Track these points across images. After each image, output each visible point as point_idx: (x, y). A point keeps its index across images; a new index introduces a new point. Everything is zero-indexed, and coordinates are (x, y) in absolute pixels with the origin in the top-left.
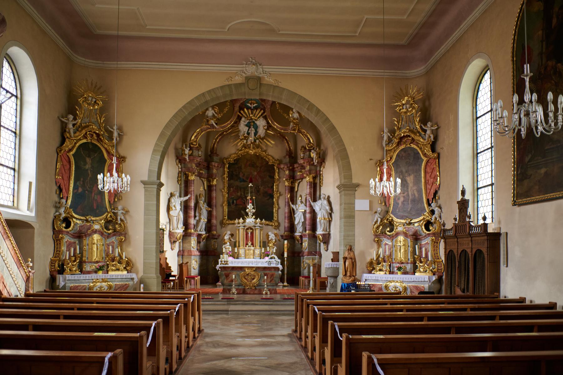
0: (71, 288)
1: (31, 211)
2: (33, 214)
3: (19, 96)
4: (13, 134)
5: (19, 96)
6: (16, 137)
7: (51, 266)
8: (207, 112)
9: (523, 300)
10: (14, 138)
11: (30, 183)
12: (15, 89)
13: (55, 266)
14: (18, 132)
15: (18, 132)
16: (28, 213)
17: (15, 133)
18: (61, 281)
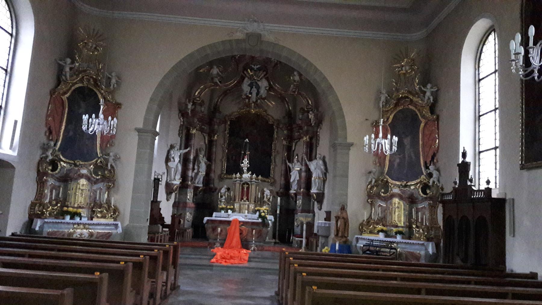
0: (48, 233)
1: (14, 151)
2: (15, 154)
3: (14, 34)
4: (4, 72)
5: (14, 34)
6: (6, 75)
7: (31, 209)
8: (212, 70)
9: (534, 276)
10: (5, 75)
11: (16, 122)
12: (11, 28)
13: (34, 209)
14: (9, 70)
15: (9, 70)
16: (10, 152)
17: (6, 71)
18: (38, 224)
